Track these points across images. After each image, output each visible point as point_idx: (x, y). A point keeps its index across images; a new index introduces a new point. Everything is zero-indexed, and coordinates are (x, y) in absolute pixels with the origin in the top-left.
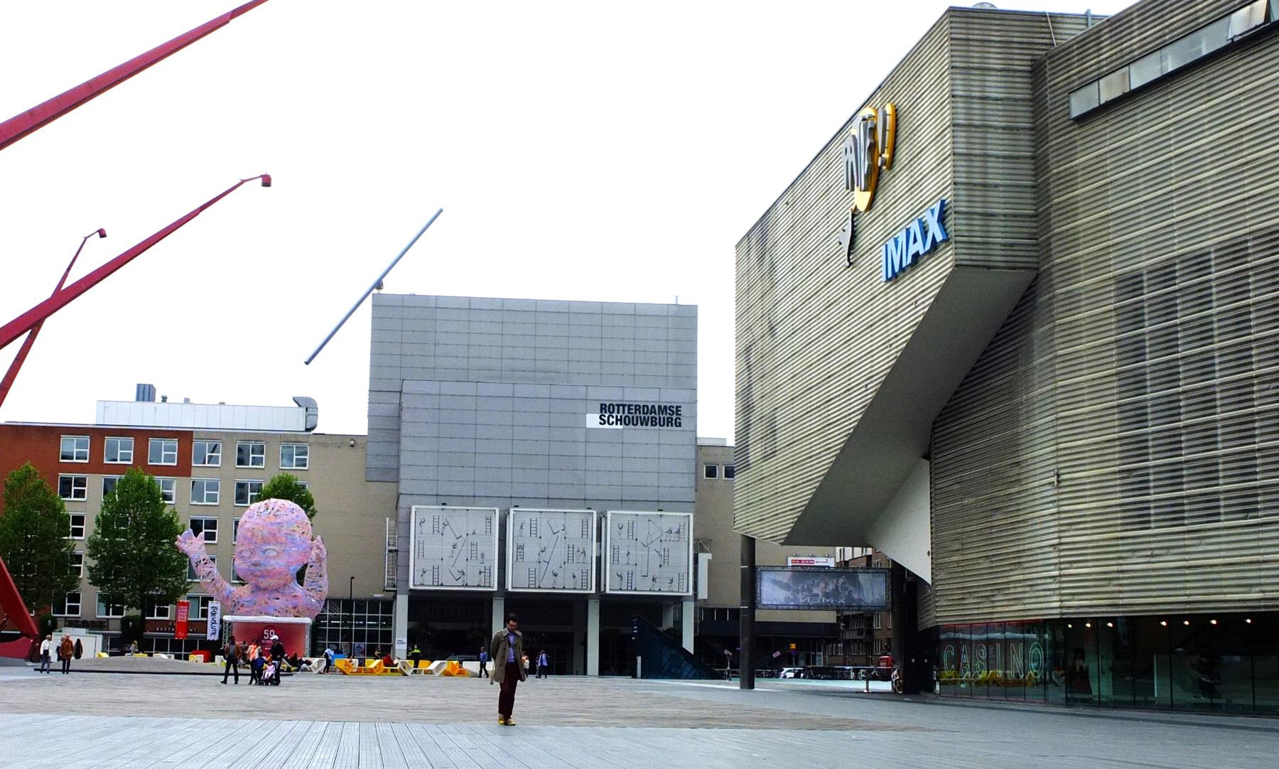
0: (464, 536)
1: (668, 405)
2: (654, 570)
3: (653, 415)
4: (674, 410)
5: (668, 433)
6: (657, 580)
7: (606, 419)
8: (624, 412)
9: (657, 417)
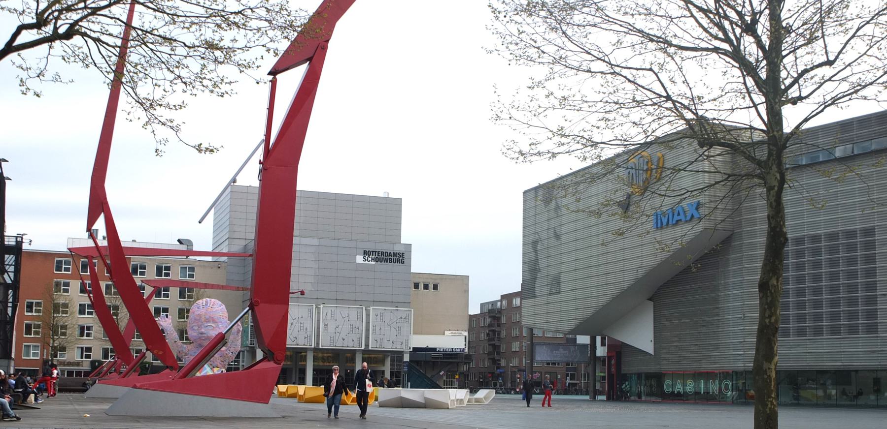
0: (297, 318)
1: (398, 252)
2: (393, 338)
3: (390, 257)
4: (401, 255)
5: (397, 267)
6: (395, 343)
7: (366, 258)
8: (375, 255)
9: (392, 258)
